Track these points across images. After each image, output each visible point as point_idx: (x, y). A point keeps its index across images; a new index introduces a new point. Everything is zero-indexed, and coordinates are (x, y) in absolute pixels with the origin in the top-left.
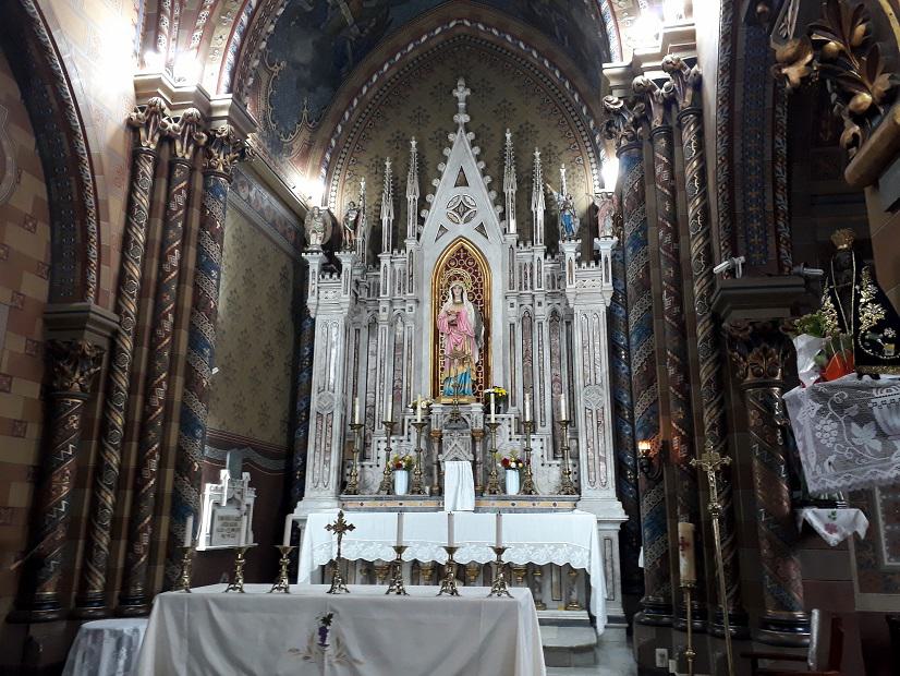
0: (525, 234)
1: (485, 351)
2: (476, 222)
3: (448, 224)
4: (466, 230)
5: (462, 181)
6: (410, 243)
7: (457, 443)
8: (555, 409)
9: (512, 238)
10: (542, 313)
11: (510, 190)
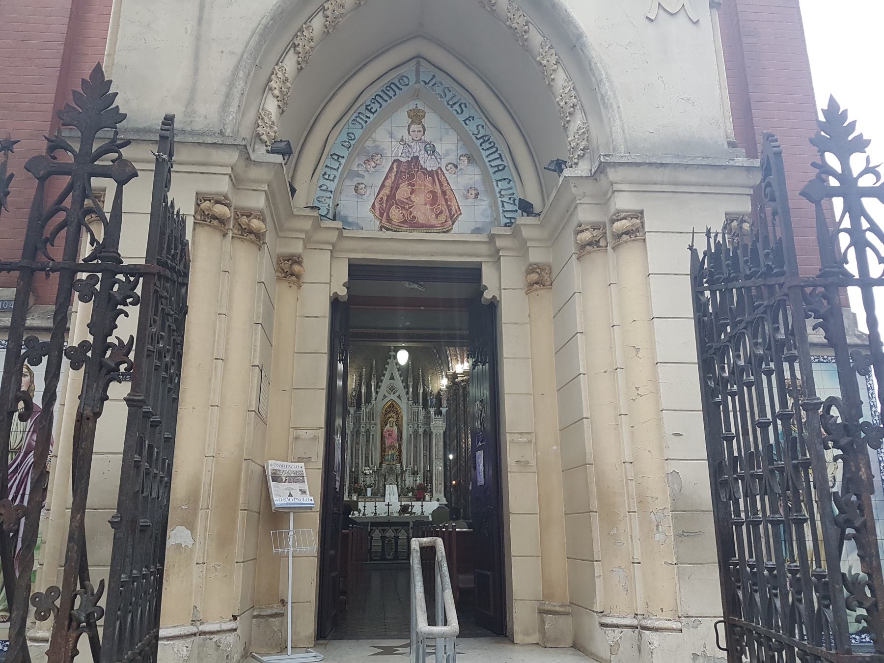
0: (416, 402)
1: (400, 445)
2: (397, 394)
3: (387, 394)
4: (392, 397)
5: (392, 378)
6: (373, 402)
7: (392, 478)
8: (425, 467)
9: (411, 402)
10: (421, 431)
11: (411, 384)
